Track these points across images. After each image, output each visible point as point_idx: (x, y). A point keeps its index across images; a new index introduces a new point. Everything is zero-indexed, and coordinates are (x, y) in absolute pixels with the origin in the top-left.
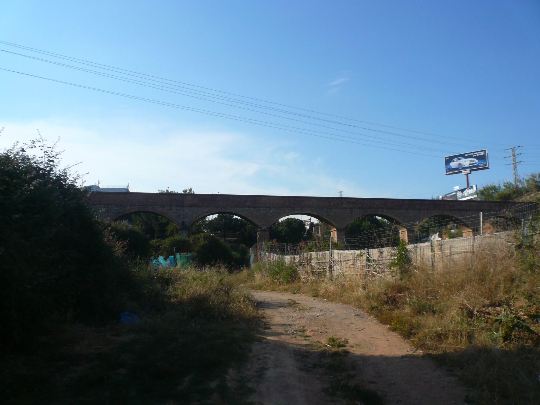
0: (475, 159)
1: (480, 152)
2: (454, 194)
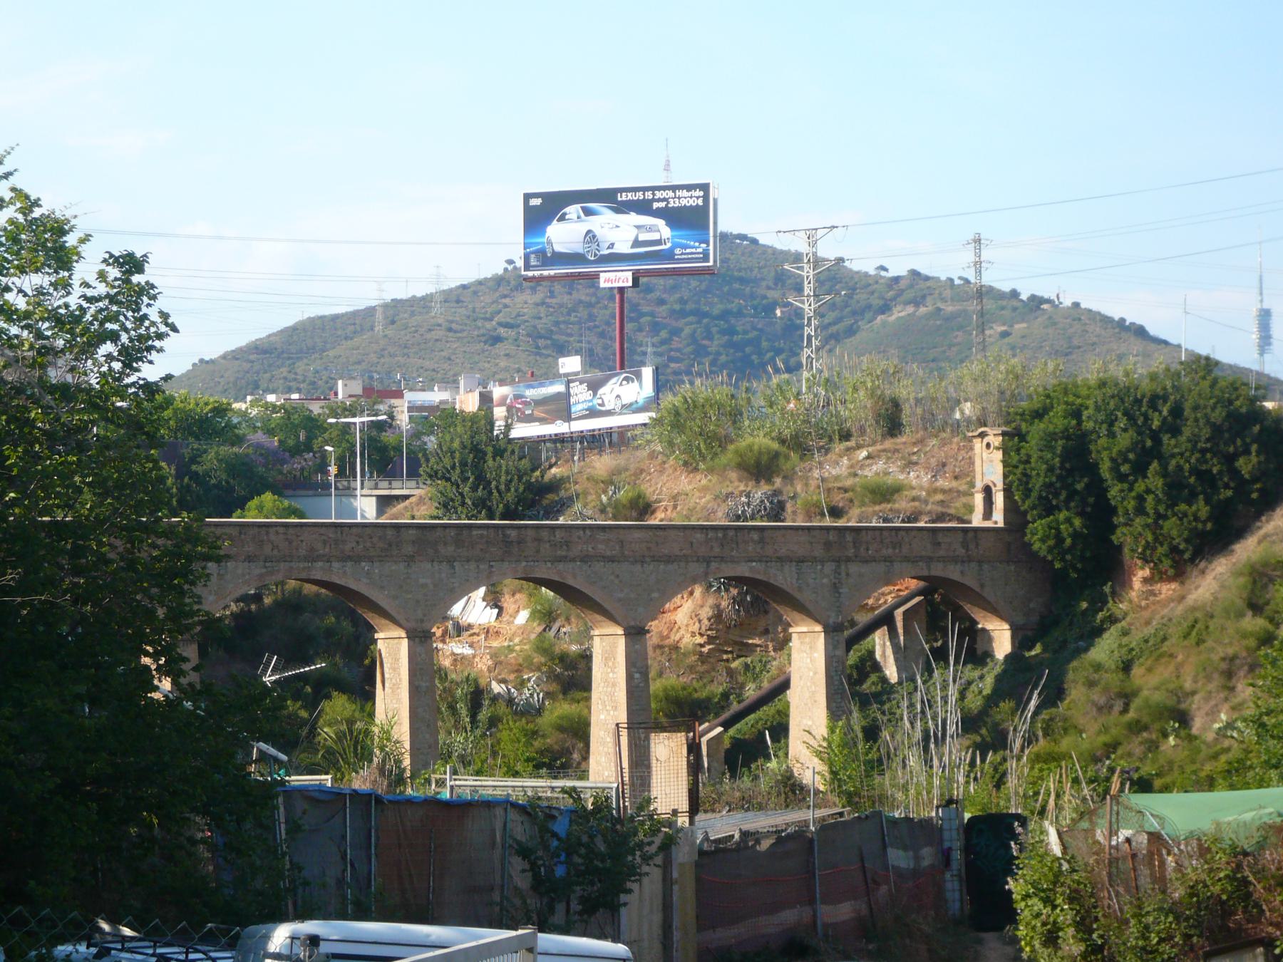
0: (660, 223)
1: (685, 193)
2: (559, 394)
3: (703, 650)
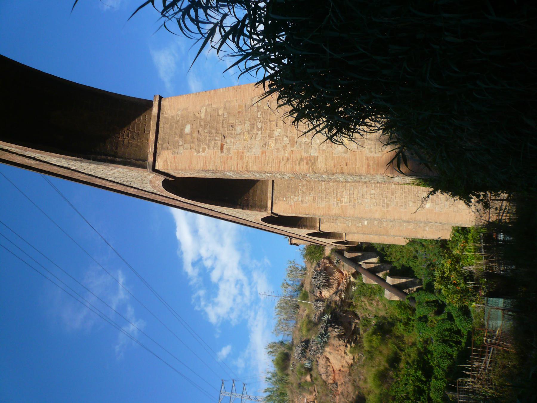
3: (353, 347)
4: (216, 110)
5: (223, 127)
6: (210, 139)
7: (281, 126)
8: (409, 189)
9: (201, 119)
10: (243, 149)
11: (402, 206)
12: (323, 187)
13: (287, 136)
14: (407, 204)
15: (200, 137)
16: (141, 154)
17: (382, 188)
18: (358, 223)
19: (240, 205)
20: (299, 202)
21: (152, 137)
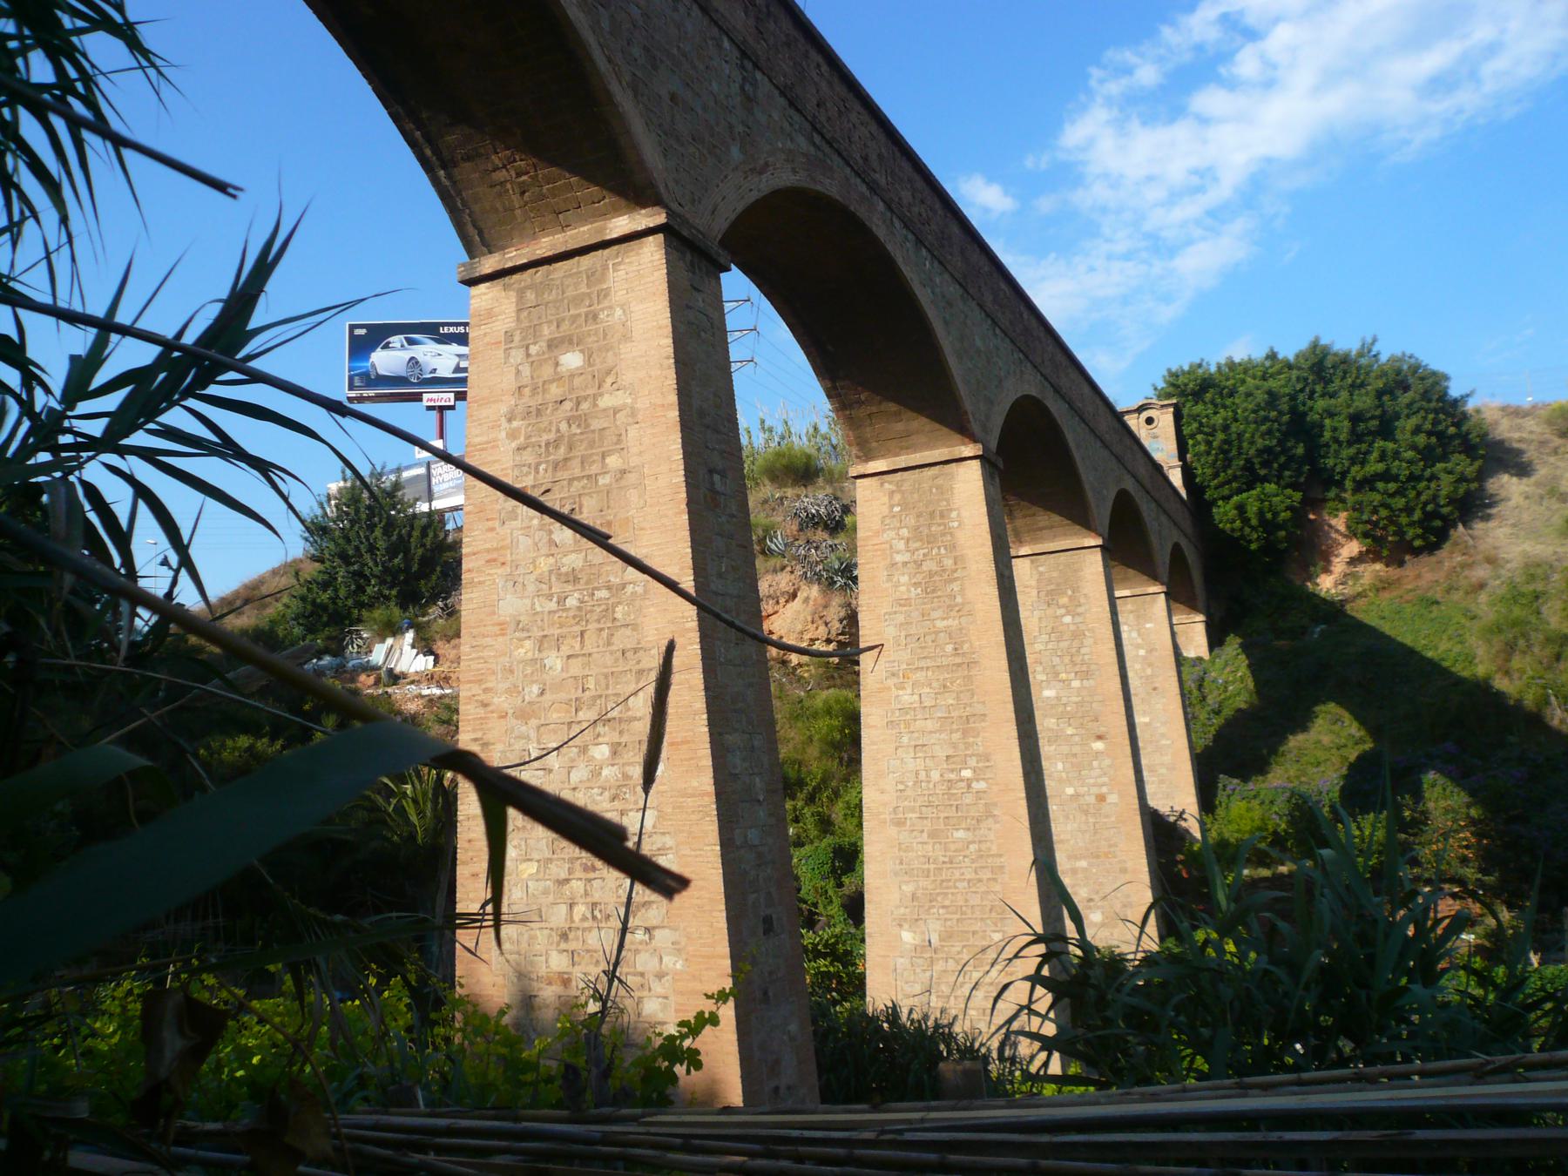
4: (619, 445)
5: (571, 481)
6: (540, 446)
7: (567, 672)
8: (950, 880)
9: (595, 397)
10: (512, 561)
11: (901, 863)
12: (940, 624)
13: (542, 694)
14: (906, 878)
15: (549, 411)
16: (497, 228)
17: (947, 803)
18: (1044, 669)
19: (835, 388)
20: (891, 556)
21: (547, 245)
